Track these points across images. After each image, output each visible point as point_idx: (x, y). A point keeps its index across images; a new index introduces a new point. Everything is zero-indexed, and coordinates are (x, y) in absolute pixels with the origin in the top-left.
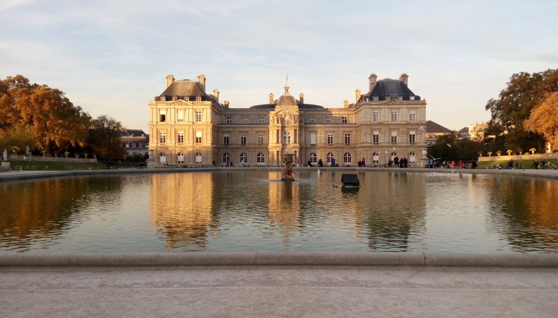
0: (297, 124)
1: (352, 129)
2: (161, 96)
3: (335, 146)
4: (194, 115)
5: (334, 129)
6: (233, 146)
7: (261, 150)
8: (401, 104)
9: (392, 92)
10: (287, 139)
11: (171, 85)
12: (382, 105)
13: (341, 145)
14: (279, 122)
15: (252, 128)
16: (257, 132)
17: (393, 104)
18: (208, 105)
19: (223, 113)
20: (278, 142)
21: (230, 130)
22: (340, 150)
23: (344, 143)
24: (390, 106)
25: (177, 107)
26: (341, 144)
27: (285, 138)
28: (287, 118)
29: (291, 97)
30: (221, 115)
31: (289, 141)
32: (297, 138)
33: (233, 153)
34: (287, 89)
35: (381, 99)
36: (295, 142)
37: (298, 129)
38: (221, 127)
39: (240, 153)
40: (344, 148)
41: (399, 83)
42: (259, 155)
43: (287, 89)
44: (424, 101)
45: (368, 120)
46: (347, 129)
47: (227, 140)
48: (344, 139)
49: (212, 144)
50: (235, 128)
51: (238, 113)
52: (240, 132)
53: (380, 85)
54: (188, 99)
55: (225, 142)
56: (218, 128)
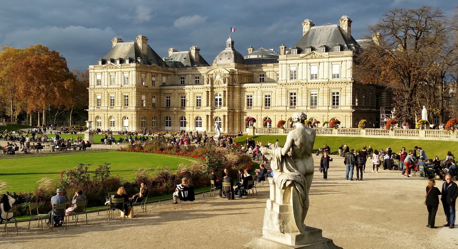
0: (226, 85)
3: (273, 109)
6: (173, 109)
8: (321, 57)
9: (319, 42)
10: (218, 102)
14: (210, 82)
17: (312, 58)
18: (133, 67)
19: (176, 73)
20: (208, 105)
21: (171, 91)
24: (309, 61)
25: (109, 70)
27: (217, 100)
28: (218, 77)
30: (175, 75)
31: (220, 104)
32: (226, 100)
33: (173, 116)
35: (300, 51)
36: (225, 105)
37: (226, 90)
39: (180, 116)
41: (333, 30)
42: (197, 119)
47: (168, 102)
49: (136, 107)
50: (175, 90)
52: (179, 94)
53: (310, 34)
54: (118, 62)
55: (167, 105)
56: (160, 90)
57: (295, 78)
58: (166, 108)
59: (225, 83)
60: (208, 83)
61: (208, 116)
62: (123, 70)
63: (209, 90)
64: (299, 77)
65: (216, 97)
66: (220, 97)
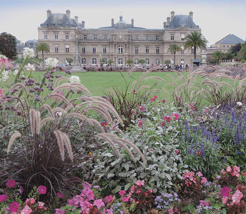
0: (126, 41)
1: (160, 44)
2: (44, 24)
4: (65, 35)
5: (149, 44)
7: (105, 56)
9: (183, 23)
11: (49, 17)
12: (176, 31)
13: (154, 54)
14: (116, 39)
15: (99, 43)
16: (102, 45)
17: (182, 31)
18: (72, 29)
20: (115, 52)
22: (153, 57)
23: (156, 52)
26: (153, 53)
27: (119, 49)
28: (121, 37)
29: (123, 23)
34: (121, 18)
38: (80, 42)
39: (92, 58)
40: (155, 56)
43: (121, 18)
44: (200, 29)
45: (167, 39)
46: (157, 44)
48: (156, 51)
51: (91, 33)
53: (177, 18)
57: (173, 40)
58: (83, 53)
59: (126, 40)
60: (115, 40)
61: (115, 58)
62: (65, 30)
63: (116, 43)
64: (175, 39)
65: (119, 48)
66: (122, 48)
